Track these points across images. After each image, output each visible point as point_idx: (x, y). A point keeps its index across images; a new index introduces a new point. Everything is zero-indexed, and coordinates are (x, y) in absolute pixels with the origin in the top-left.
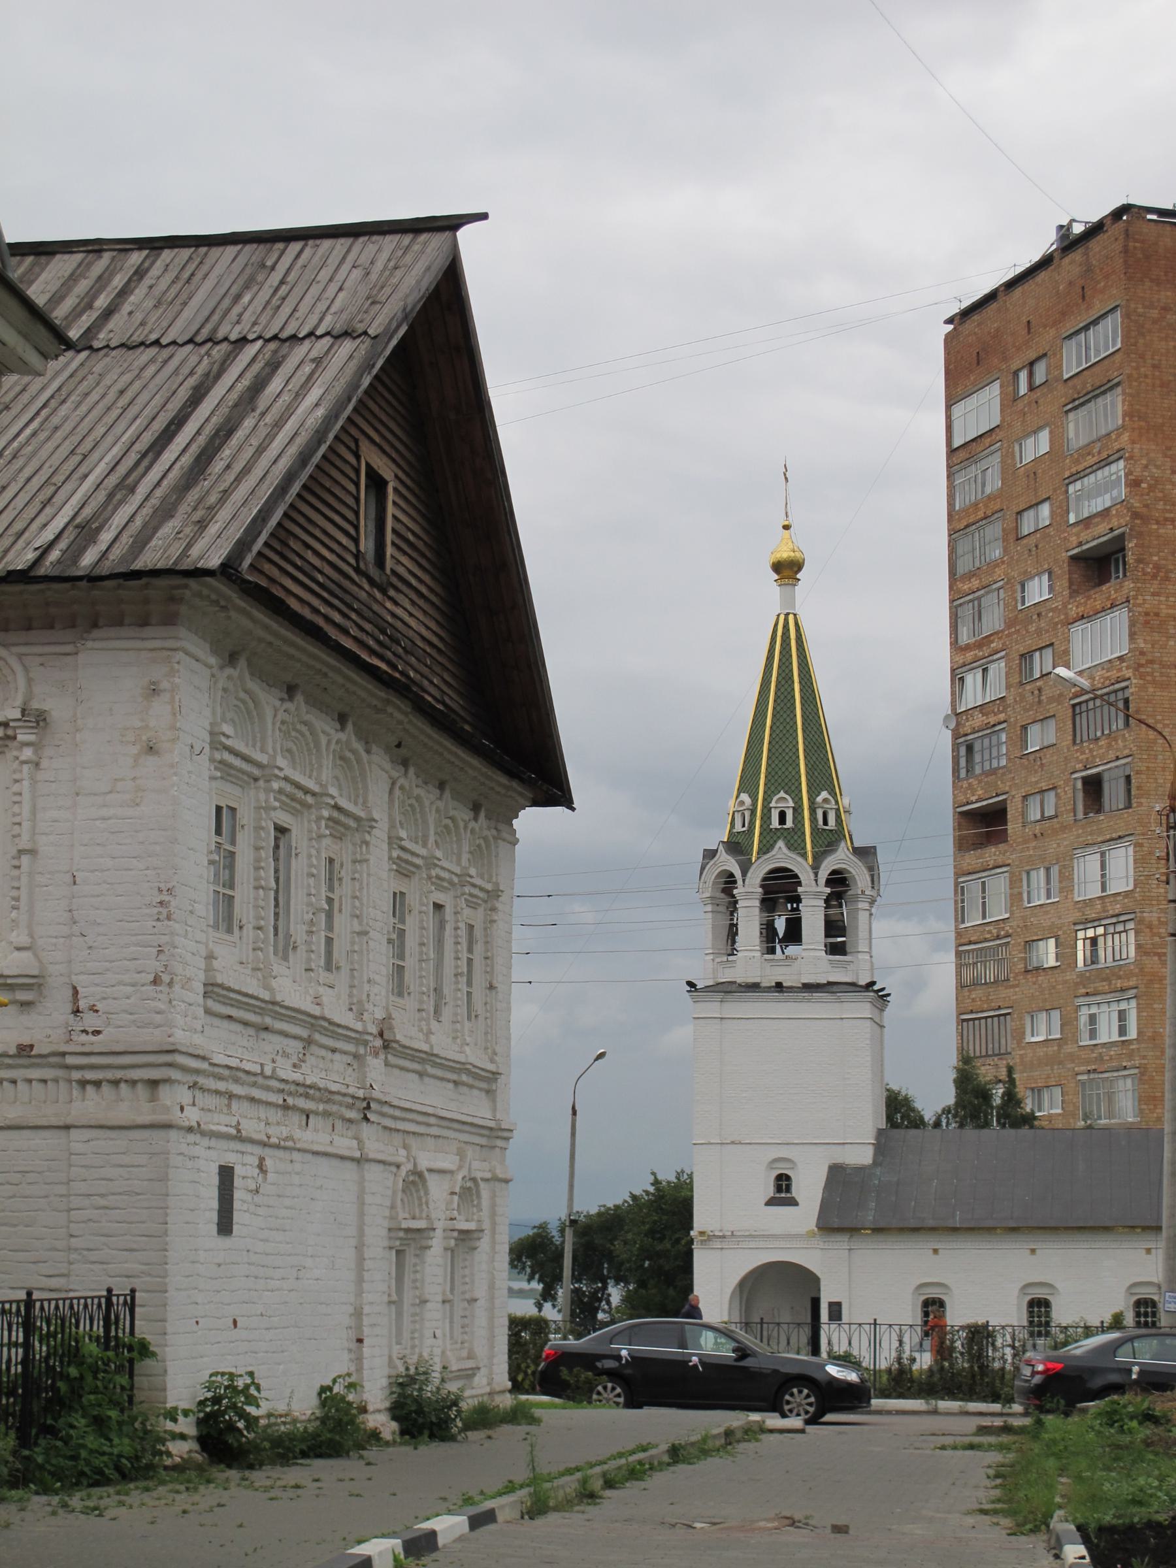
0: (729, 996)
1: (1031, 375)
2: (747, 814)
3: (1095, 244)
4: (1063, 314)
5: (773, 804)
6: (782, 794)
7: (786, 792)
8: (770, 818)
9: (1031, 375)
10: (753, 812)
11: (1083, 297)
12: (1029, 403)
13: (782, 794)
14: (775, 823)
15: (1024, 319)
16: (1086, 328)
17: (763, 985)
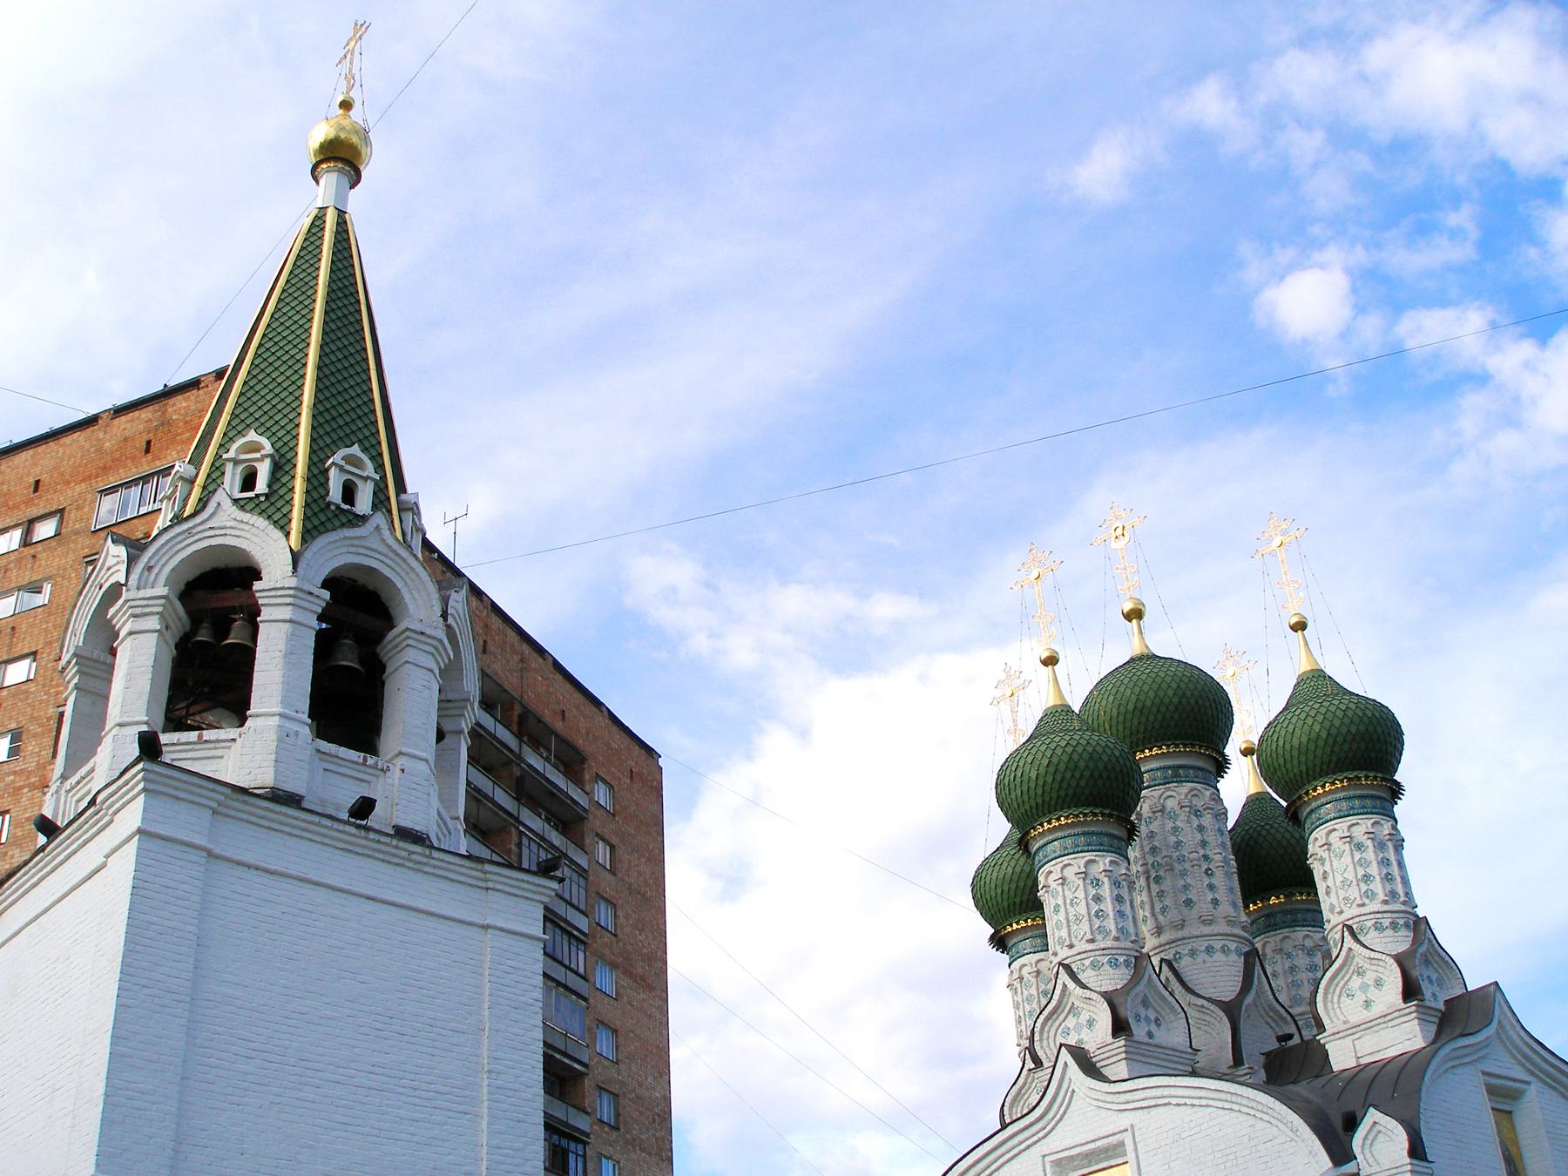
0: (238, 803)
1: (28, 532)
2: (264, 471)
3: (180, 402)
4: (106, 469)
5: (337, 458)
6: (355, 450)
7: (365, 450)
8: (325, 484)
9: (28, 532)
10: (282, 466)
11: (147, 451)
12: (19, 560)
13: (355, 450)
14: (335, 493)
15: (32, 480)
16: (145, 479)
17: (305, 804)
